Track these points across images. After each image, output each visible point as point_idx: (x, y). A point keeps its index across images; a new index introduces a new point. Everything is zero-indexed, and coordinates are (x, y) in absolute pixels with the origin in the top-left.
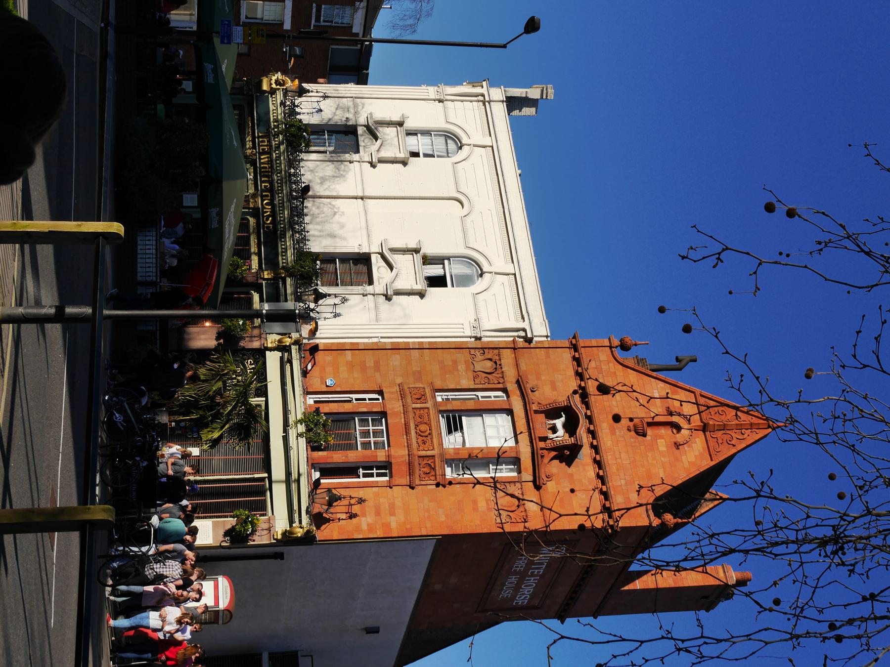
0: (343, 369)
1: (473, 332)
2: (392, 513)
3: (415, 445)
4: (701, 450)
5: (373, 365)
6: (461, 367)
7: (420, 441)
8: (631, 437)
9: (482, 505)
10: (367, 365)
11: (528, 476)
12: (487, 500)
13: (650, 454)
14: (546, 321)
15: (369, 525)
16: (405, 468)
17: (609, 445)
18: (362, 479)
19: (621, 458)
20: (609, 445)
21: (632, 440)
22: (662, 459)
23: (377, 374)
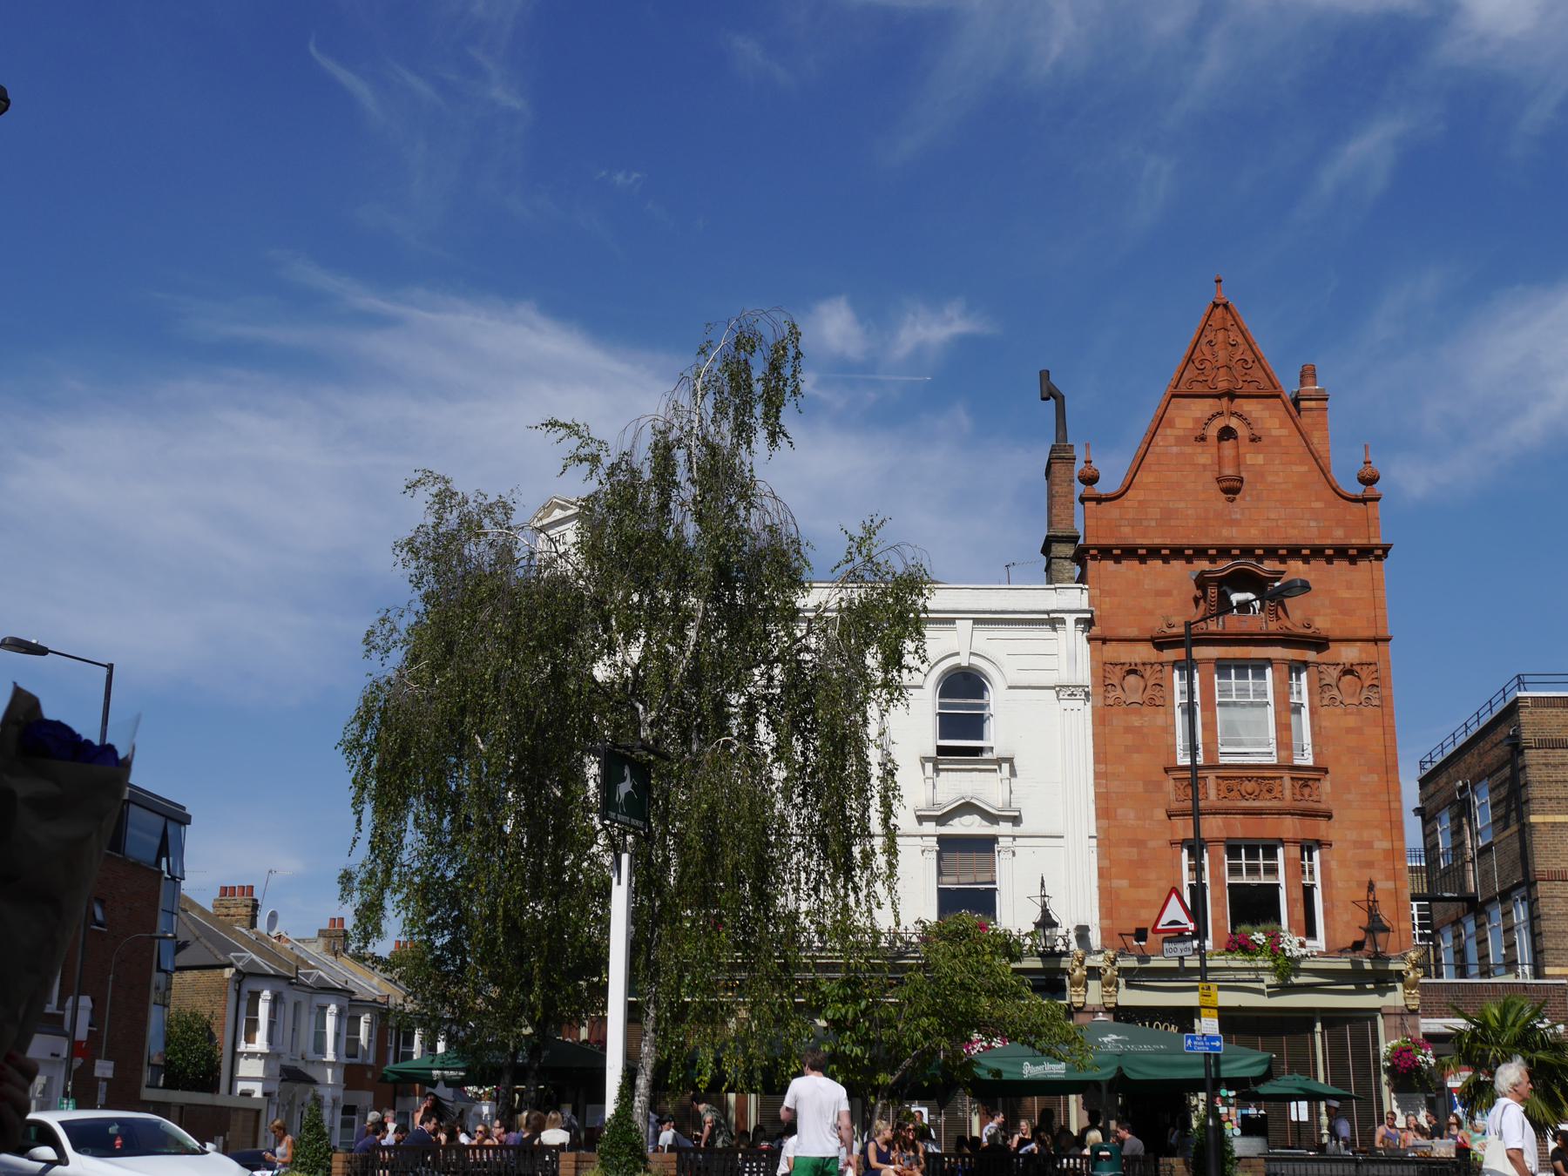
0: (1142, 894)
1: (1078, 697)
2: (1368, 845)
3: (1275, 804)
4: (1260, 406)
5: (1135, 850)
6: (1136, 721)
7: (1268, 796)
8: (1243, 499)
9: (1351, 721)
10: (1136, 858)
11: (1311, 656)
12: (1346, 714)
13: (1270, 479)
14: (1057, 585)
15: (1387, 879)
16: (1308, 821)
17: (1256, 532)
18: (1281, 879)
19: (1277, 520)
20: (1256, 532)
21: (1248, 499)
22: (1277, 462)
23: (1151, 844)
